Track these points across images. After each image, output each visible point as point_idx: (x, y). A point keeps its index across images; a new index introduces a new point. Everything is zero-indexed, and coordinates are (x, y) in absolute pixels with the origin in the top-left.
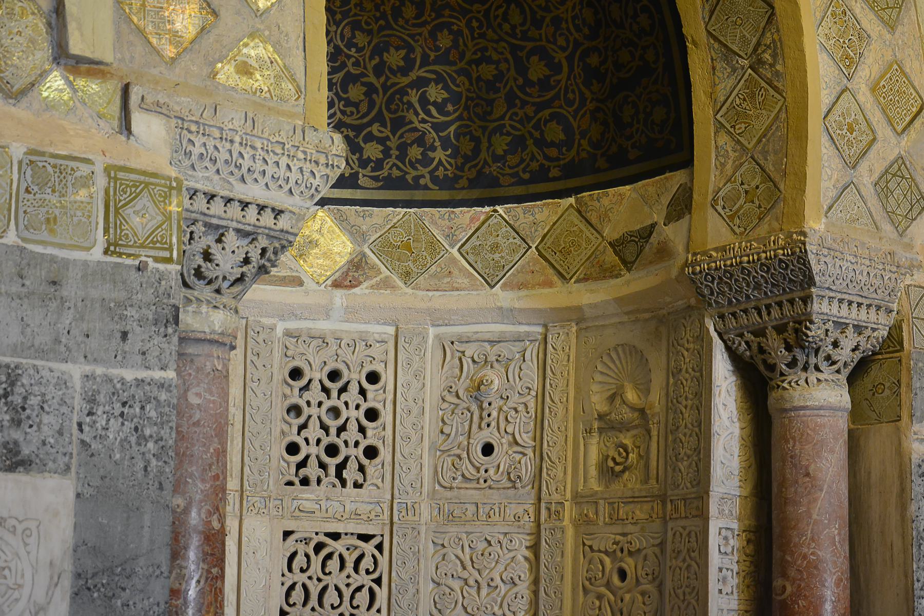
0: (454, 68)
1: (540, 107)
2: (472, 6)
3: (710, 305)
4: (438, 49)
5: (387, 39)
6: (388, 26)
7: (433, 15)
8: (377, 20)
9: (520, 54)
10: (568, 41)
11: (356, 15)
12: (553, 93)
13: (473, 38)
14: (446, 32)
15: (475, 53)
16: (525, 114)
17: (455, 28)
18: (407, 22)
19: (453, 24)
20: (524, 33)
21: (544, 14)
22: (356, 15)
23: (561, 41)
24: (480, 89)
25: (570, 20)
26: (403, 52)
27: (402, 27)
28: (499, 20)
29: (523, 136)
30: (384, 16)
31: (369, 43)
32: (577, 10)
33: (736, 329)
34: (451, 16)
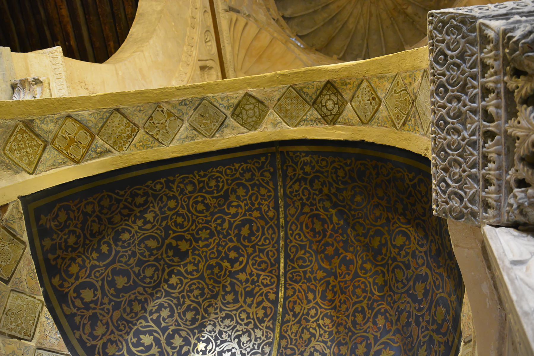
0: (391, 333)
1: (429, 309)
2: (383, 291)
3: (474, 214)
4: (379, 328)
5: (355, 341)
6: (354, 334)
7: (370, 311)
8: (347, 334)
9: (410, 292)
10: (423, 258)
11: (338, 338)
12: (430, 293)
13: (392, 307)
14: (379, 316)
15: (396, 315)
16: (426, 321)
17: (383, 310)
18: (361, 326)
19: (381, 309)
20: (407, 279)
21: (407, 258)
22: (338, 338)
23: (420, 261)
24: (405, 333)
25: (417, 246)
26: (364, 343)
27: (360, 329)
28: (396, 285)
29: (431, 337)
30: (350, 330)
31: (347, 350)
32: (417, 238)
33: (498, 192)
34: (378, 305)
